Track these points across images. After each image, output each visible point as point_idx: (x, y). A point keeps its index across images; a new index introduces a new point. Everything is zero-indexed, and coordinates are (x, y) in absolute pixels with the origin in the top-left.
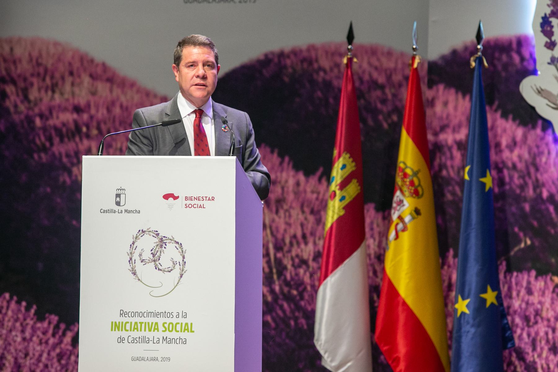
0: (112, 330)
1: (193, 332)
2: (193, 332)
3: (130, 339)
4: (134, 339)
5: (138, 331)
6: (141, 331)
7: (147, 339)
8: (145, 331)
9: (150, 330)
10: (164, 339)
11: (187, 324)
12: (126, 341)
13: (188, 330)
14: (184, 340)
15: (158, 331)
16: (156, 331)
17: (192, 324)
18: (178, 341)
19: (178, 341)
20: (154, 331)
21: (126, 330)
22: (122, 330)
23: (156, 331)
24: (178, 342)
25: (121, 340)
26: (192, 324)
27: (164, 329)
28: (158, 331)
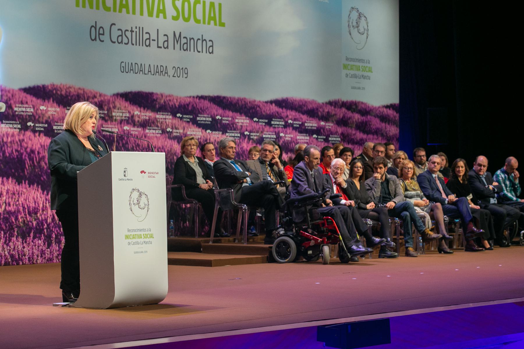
0: (77, 5)
1: (222, 25)
2: (222, 25)
3: (115, 34)
4: (123, 33)
5: (128, 12)
6: (134, 13)
7: (146, 36)
8: (142, 14)
9: (150, 14)
10: (177, 38)
11: (212, 4)
12: (106, 38)
13: (214, 19)
14: (209, 44)
15: (165, 17)
16: (161, 15)
17: (220, 5)
20: (158, 16)
21: (107, 9)
22: (98, 8)
23: (161, 15)
25: (97, 33)
26: (220, 5)
27: (175, 14)
28: (165, 17)
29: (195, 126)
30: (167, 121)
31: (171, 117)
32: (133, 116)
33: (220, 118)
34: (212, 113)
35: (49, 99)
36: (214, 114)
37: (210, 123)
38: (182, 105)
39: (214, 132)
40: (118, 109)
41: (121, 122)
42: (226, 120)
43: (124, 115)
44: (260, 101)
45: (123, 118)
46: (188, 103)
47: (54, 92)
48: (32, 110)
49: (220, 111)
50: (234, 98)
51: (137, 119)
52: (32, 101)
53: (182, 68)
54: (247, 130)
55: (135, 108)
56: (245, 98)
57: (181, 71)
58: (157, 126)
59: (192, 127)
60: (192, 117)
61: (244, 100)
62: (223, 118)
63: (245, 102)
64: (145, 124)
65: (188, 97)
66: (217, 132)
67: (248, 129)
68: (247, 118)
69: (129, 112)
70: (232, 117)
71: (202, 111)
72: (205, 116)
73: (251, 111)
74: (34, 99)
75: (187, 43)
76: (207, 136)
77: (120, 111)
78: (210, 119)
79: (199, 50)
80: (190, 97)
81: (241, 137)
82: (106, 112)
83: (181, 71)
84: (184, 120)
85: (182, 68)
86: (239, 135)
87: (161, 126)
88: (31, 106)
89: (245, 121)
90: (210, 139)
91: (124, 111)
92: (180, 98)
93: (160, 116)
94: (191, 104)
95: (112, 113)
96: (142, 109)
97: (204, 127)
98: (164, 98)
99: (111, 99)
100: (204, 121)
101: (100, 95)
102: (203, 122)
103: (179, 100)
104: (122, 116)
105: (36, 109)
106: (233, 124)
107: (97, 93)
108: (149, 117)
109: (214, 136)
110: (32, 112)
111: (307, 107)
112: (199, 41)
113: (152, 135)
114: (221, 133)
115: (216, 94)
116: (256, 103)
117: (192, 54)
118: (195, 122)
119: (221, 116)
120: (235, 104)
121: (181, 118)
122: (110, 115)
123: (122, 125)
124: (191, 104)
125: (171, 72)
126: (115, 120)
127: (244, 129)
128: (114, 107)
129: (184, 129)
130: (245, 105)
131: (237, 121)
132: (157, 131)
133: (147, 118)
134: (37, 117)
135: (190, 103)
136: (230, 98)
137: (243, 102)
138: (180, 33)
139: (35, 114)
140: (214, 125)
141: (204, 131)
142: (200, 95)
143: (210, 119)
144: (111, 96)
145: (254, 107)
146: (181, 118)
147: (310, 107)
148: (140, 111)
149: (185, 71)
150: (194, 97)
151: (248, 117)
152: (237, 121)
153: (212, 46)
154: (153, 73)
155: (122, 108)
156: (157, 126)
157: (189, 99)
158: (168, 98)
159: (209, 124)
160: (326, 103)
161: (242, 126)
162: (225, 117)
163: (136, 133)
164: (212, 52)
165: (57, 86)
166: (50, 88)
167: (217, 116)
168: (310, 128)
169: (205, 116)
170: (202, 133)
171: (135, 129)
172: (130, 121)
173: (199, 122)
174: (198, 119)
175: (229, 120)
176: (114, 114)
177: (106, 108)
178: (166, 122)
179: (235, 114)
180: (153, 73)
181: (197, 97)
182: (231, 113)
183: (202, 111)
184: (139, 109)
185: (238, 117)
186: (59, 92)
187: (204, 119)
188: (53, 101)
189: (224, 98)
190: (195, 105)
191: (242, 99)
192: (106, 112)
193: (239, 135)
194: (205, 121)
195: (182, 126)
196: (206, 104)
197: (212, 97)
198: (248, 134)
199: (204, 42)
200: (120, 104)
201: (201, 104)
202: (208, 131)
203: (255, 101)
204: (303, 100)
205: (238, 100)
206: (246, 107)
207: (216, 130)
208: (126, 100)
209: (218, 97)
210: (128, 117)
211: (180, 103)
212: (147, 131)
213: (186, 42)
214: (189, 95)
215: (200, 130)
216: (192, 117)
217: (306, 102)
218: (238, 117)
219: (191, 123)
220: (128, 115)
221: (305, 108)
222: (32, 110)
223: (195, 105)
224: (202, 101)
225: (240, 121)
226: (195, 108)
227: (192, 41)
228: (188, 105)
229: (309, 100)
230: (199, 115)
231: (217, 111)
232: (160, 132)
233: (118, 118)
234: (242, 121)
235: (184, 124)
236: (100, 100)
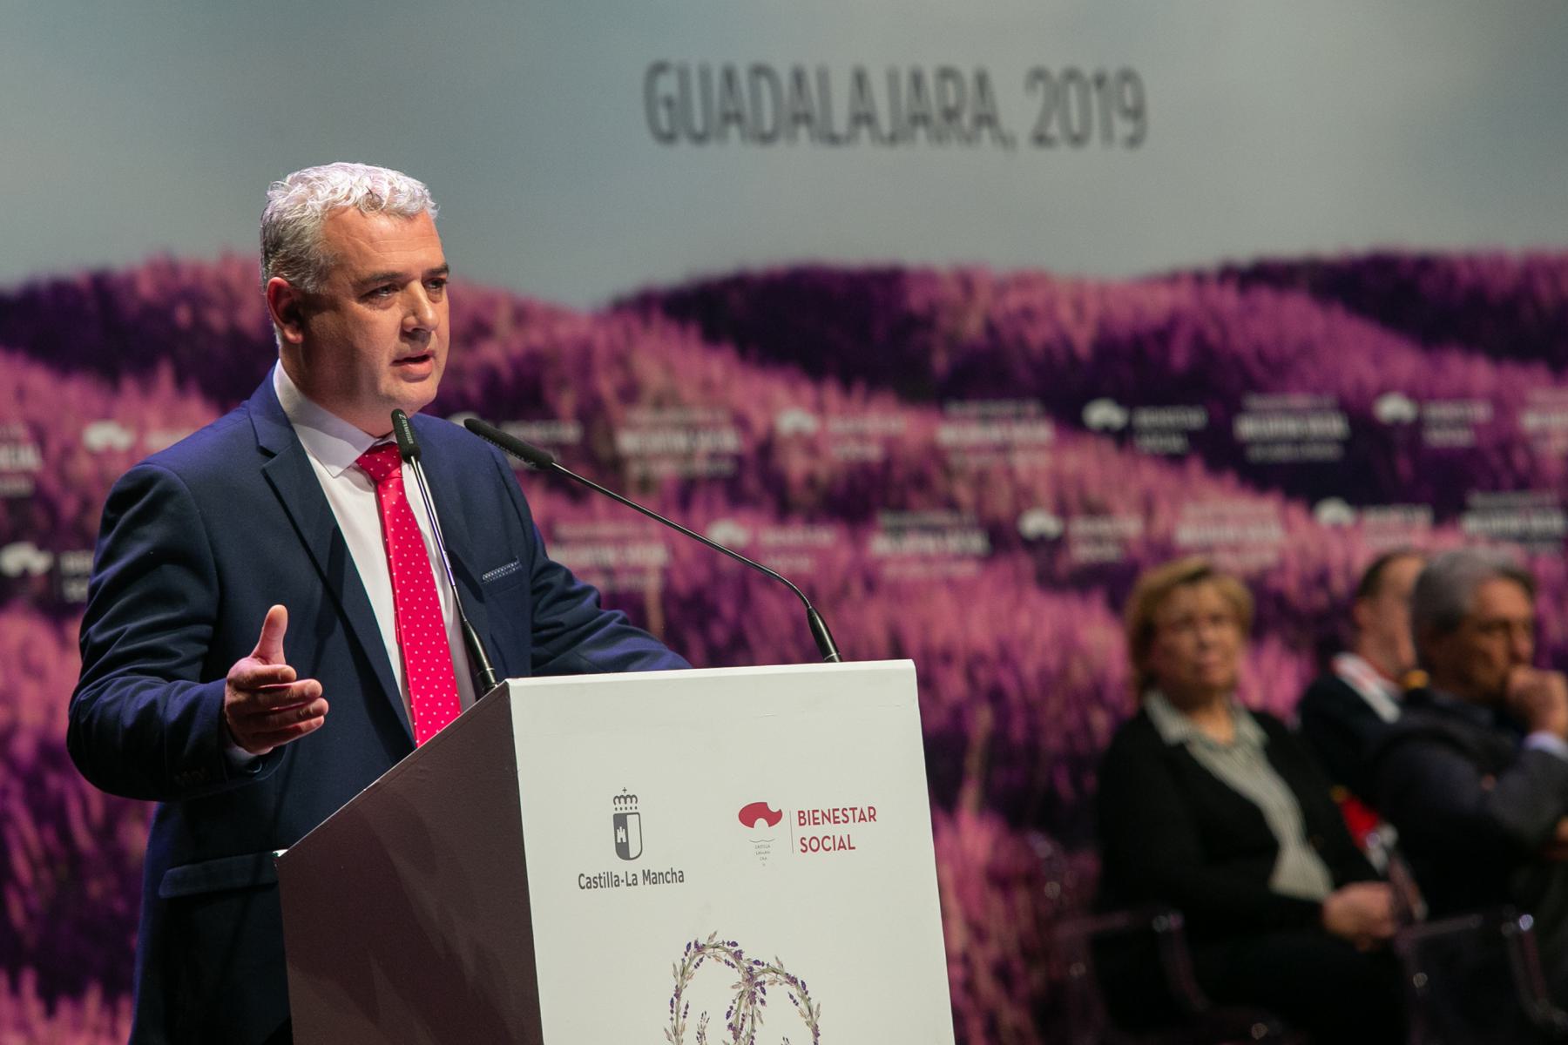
30: (1021, 462)
31: (1043, 432)
32: (766, 449)
35: (144, 369)
40: (659, 403)
41: (687, 493)
42: (1452, 425)
43: (705, 442)
45: (701, 466)
47: (183, 315)
48: (29, 458)
49: (1406, 362)
51: (796, 465)
52: (21, 394)
55: (777, 389)
58: (952, 505)
64: (858, 498)
69: (741, 422)
74: (39, 380)
77: (671, 415)
82: (570, 432)
87: (979, 505)
88: (19, 430)
91: (699, 415)
93: (963, 433)
95: (610, 437)
96: (832, 394)
97: (1297, 481)
98: (983, 298)
99: (601, 339)
101: (522, 315)
103: (1093, 308)
104: (688, 456)
105: (54, 447)
107: (491, 303)
108: (890, 443)
110: (26, 474)
113: (915, 571)
118: (1221, 455)
119: (1412, 394)
121: (1123, 437)
122: (603, 451)
123: (697, 515)
125: (1019, 109)
126: (645, 484)
128: (630, 393)
132: (954, 543)
133: (873, 452)
134: (69, 507)
135: (1174, 321)
136: (1471, 262)
139: (52, 484)
140: (1373, 467)
141: (1296, 513)
144: (600, 319)
148: (820, 409)
150: (1199, 278)
154: (885, 125)
155: (689, 392)
156: (952, 505)
158: (1014, 301)
163: (804, 565)
165: (198, 272)
166: (146, 288)
170: (1288, 526)
171: (795, 535)
172: (752, 484)
176: (628, 442)
177: (567, 401)
178: (1010, 473)
179: (1516, 376)
180: (885, 125)
182: (1481, 373)
183: (1272, 372)
184: (807, 391)
186: (216, 319)
188: (181, 381)
192: (570, 432)
196: (1297, 316)
200: (669, 369)
208: (712, 337)
210: (739, 459)
212: (880, 545)
215: (1268, 507)
219: (1195, 468)
220: (729, 441)
222: (29, 458)
224: (1265, 297)
231: (1377, 360)
232: (977, 542)
233: (666, 470)
235: (1150, 475)
236: (517, 346)
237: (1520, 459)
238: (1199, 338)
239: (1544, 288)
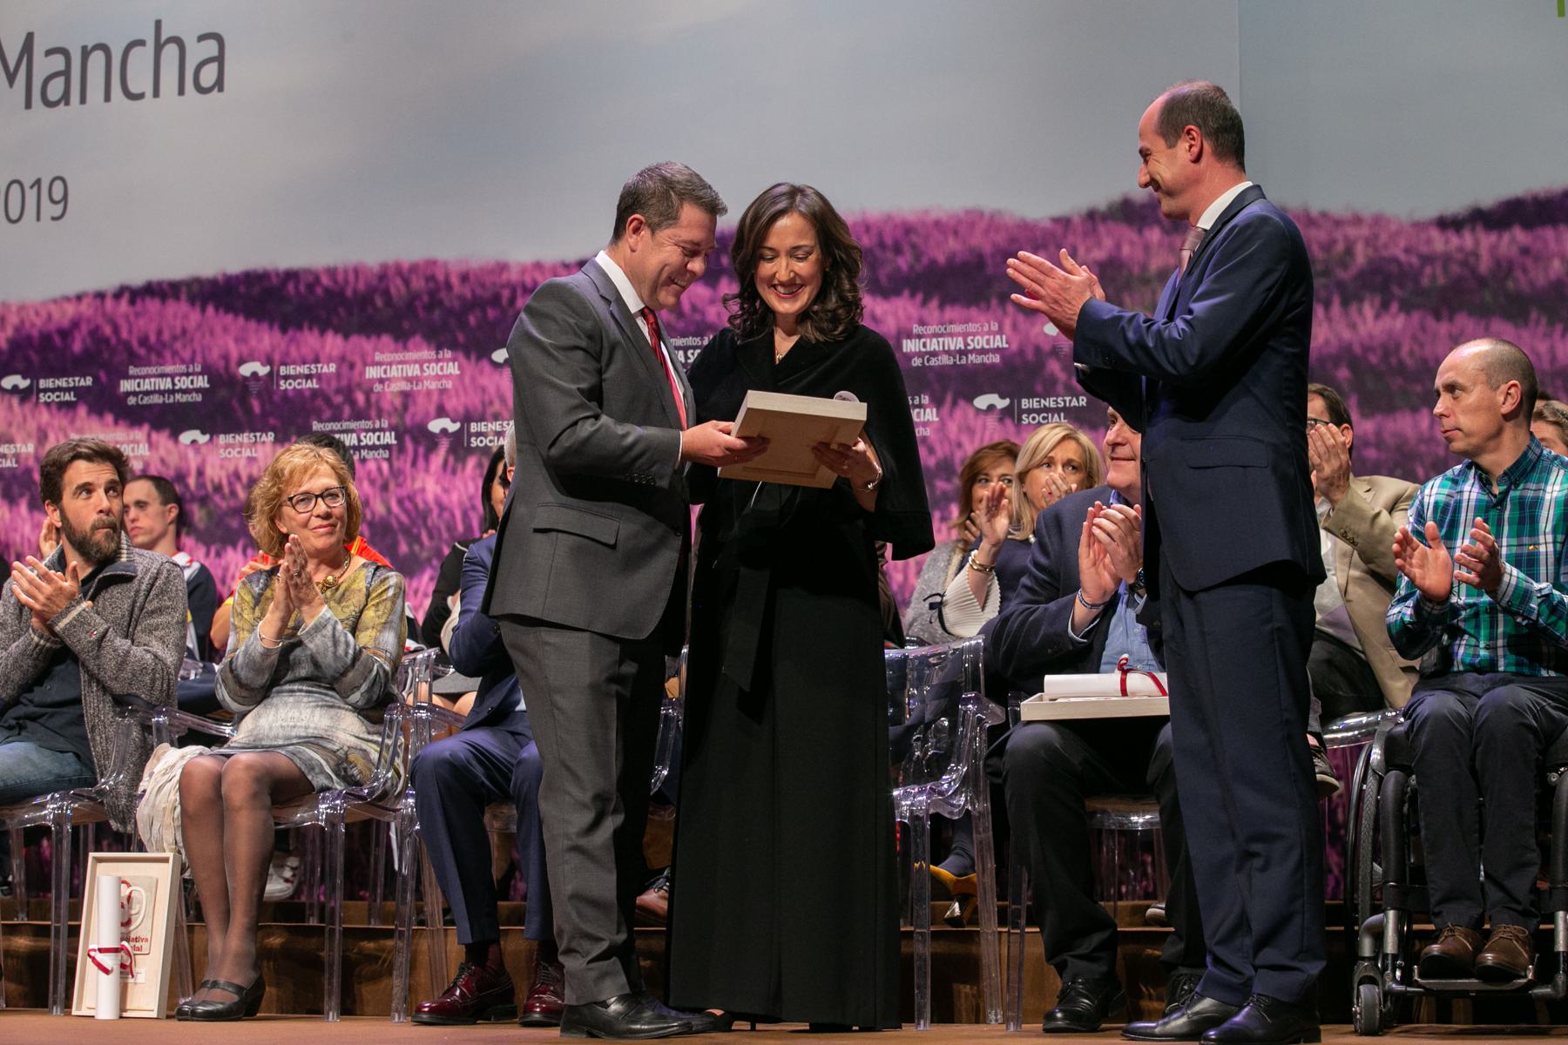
18: (141, 61)
19: (141, 61)
24: (140, 79)
29: (109, 418)
33: (263, 371)
34: (215, 355)
36: (226, 358)
37: (198, 398)
38: (29, 338)
39: (222, 439)
42: (297, 379)
44: (538, 266)
46: (66, 323)
49: (267, 338)
50: (356, 271)
53: (38, 182)
54: (441, 412)
56: (432, 263)
57: (31, 195)
59: (94, 423)
60: (89, 381)
61: (428, 270)
62: (283, 370)
63: (431, 278)
65: (67, 299)
66: (245, 438)
67: (451, 404)
68: (448, 354)
70: (342, 360)
71: (150, 349)
72: (169, 369)
73: (472, 320)
75: (66, 73)
76: (183, 457)
78: (202, 382)
79: (134, 89)
80: (79, 298)
81: (401, 448)
83: (31, 195)
84: (43, 398)
85: (38, 182)
86: (389, 438)
89: (433, 369)
90: (200, 473)
92: (22, 308)
94: (84, 328)
97: (167, 418)
100: (161, 393)
102: (157, 399)
106: (348, 393)
109: (223, 453)
111: (918, 255)
112: (136, 51)
114: (271, 436)
115: (234, 264)
116: (514, 276)
117: (98, 117)
118: (106, 402)
119: (268, 361)
120: (365, 300)
124: (84, 328)
127: (421, 406)
129: (42, 437)
130: (433, 294)
131: (372, 373)
135: (75, 324)
136: (332, 272)
137: (418, 284)
138: (30, 37)
140: (227, 406)
141: (162, 438)
142: (137, 279)
143: (202, 382)
145: (495, 300)
146: (25, 395)
147: (942, 251)
149: (54, 195)
150: (100, 296)
151: (453, 346)
152: (372, 373)
153: (220, 59)
157: (70, 310)
159: (195, 404)
160: (1092, 216)
161: (406, 396)
162: (310, 364)
164: (219, 84)
167: (241, 361)
168: (945, 360)
169: (169, 369)
173: (132, 401)
174: (126, 386)
175: (319, 377)
179: (359, 342)
181: (119, 294)
182: (333, 343)
183: (153, 350)
185: (378, 357)
187: (165, 384)
189: (291, 275)
190: (108, 330)
191: (414, 268)
193: (389, 438)
194: (172, 392)
195: (32, 426)
196: (179, 314)
197: (213, 283)
198: (453, 427)
199: (171, 52)
201: (141, 322)
202: (186, 437)
203: (502, 267)
204: (889, 218)
205: (384, 274)
206: (434, 302)
207: (237, 428)
209: (250, 278)
211: (18, 329)
213: (62, 67)
214: (72, 289)
215: (140, 434)
216: (89, 381)
217: (908, 229)
218: (378, 357)
219: (82, 411)
221: (903, 262)
223: (108, 330)
224: (153, 305)
225: (394, 372)
226: (107, 341)
227: (97, 59)
228: (66, 334)
229: (934, 215)
230: (132, 370)
234: (414, 371)
235: (45, 416)
237: (360, 398)
238: (95, 333)
239: (397, 288)
